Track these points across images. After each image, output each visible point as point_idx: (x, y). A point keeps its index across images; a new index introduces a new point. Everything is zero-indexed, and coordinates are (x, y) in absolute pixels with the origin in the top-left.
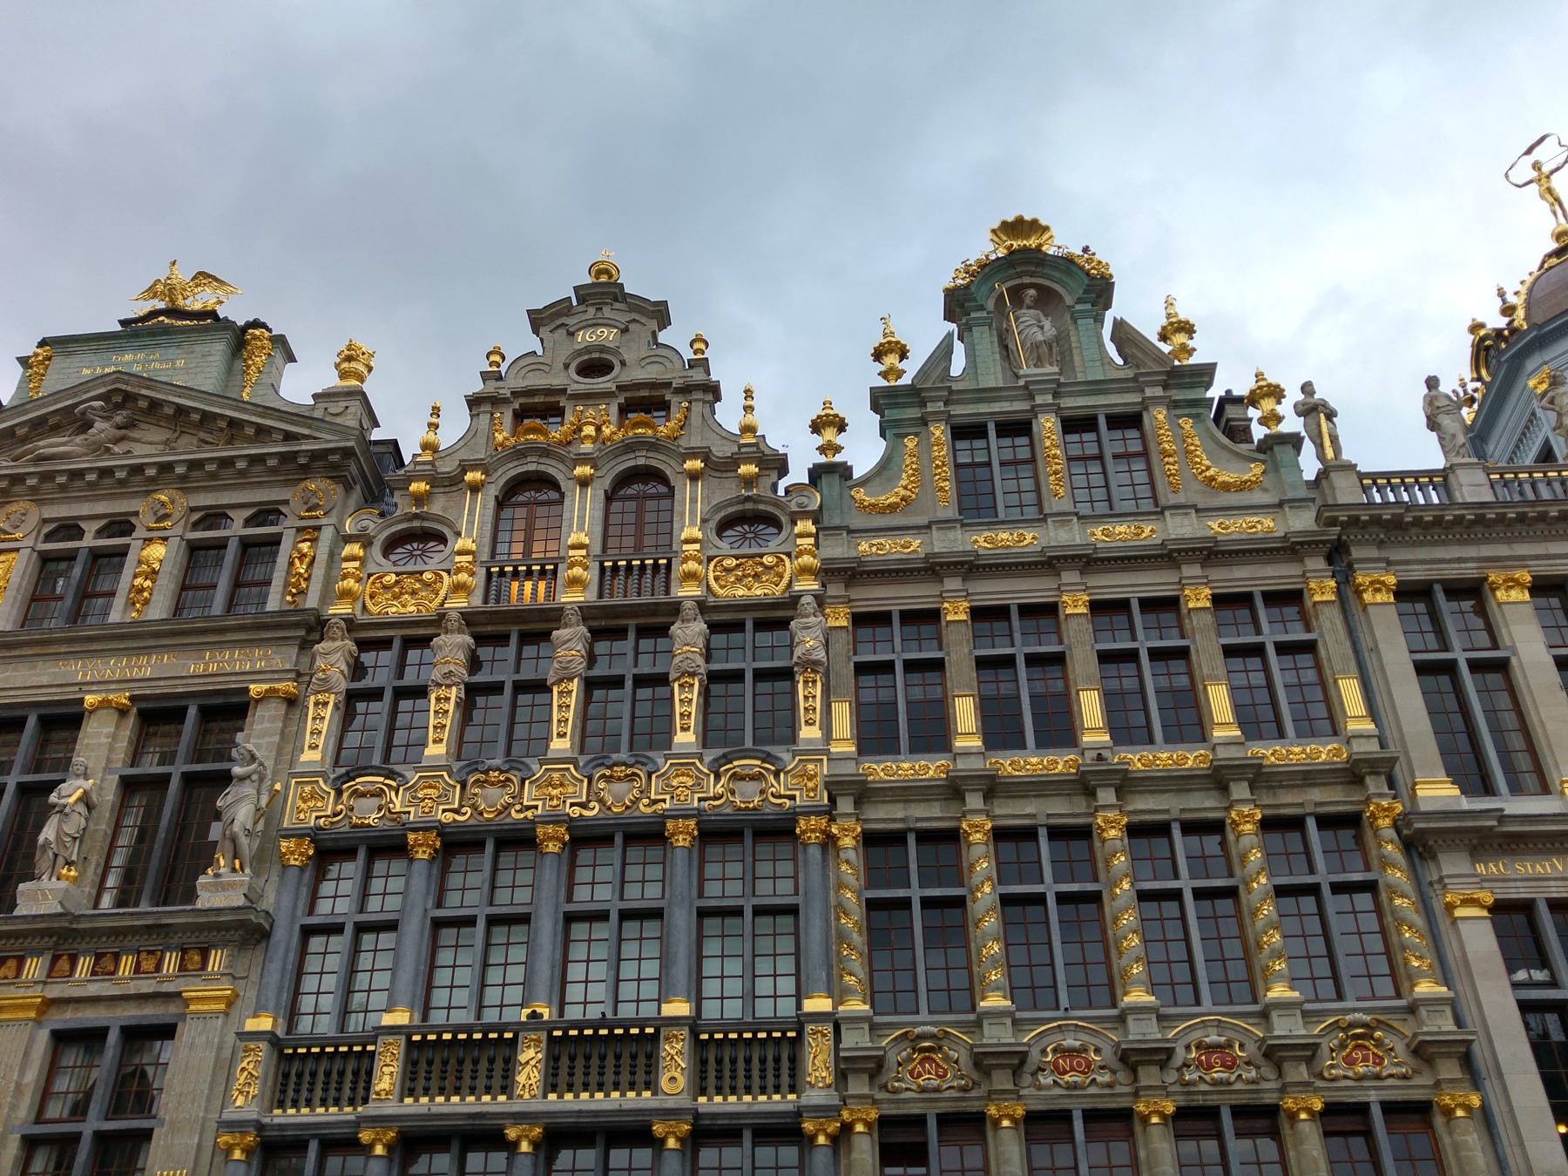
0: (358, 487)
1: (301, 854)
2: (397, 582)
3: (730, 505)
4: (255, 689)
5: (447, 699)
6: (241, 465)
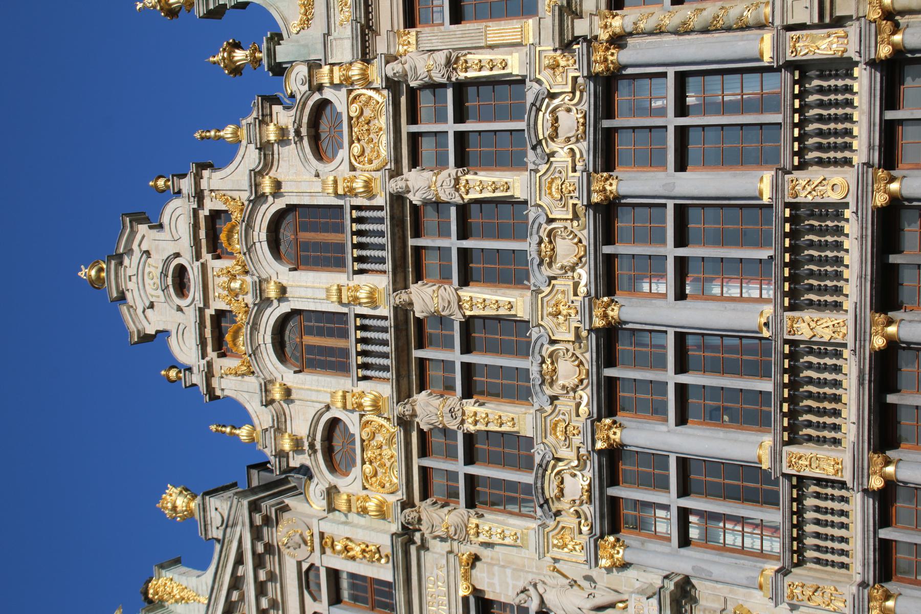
0: (287, 501)
1: (614, 547)
2: (371, 463)
3: (303, 149)
4: (463, 592)
6: (264, 603)
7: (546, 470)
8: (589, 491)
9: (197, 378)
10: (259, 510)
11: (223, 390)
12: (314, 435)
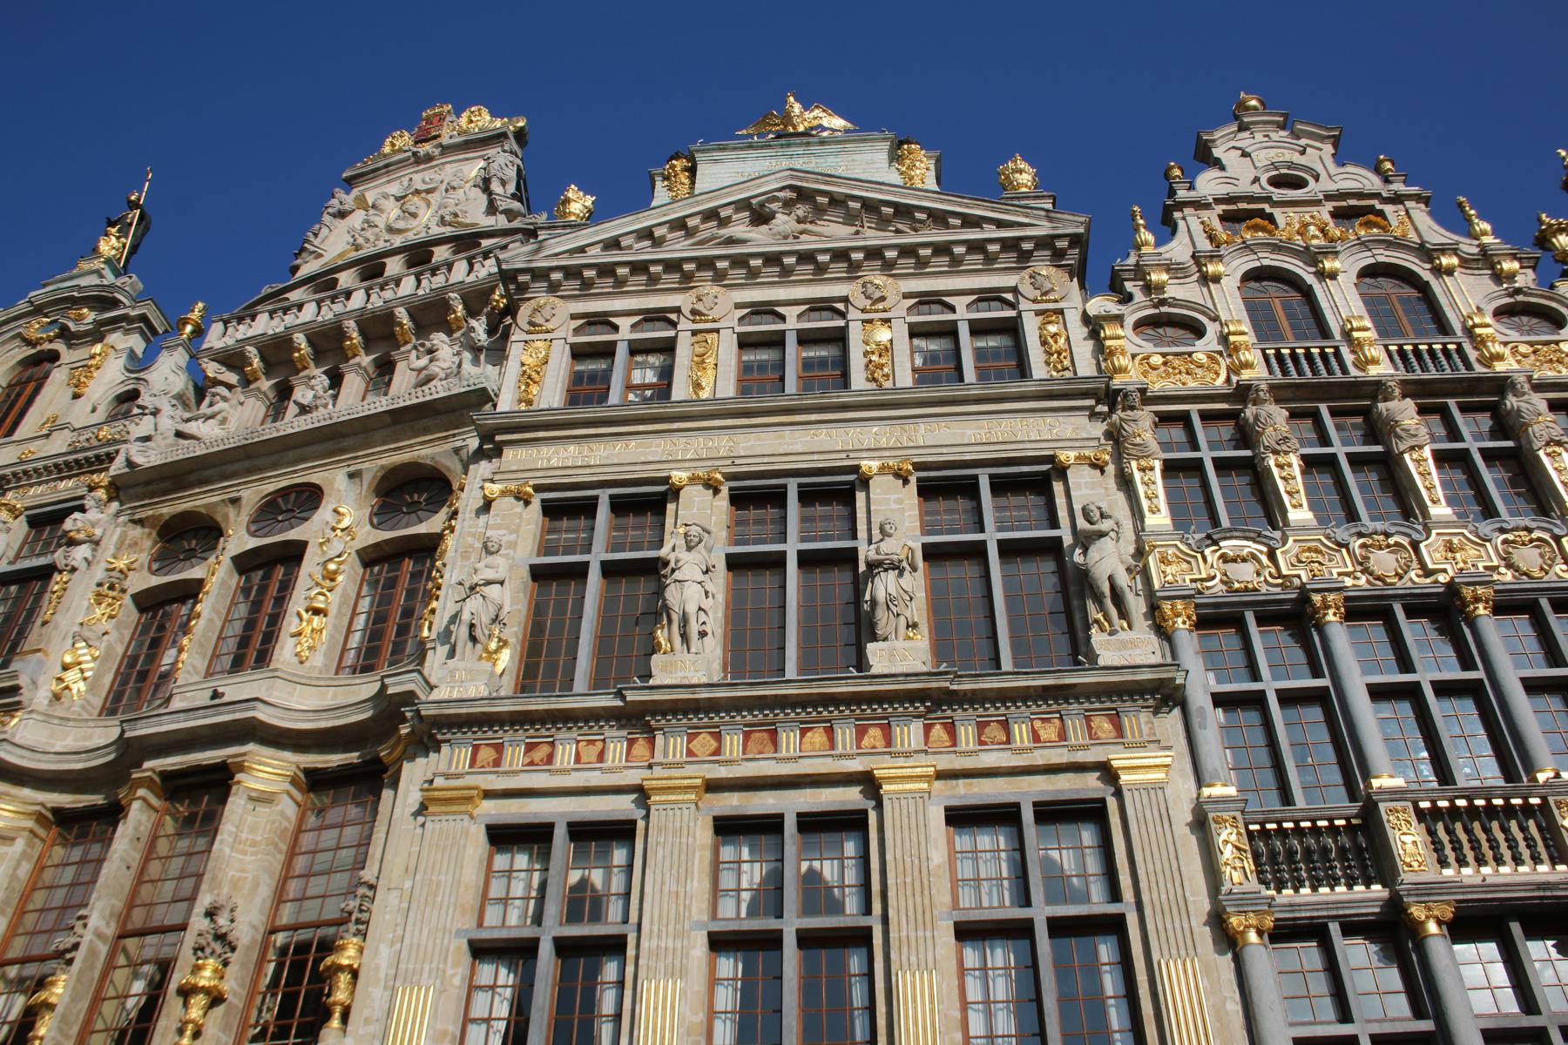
3: (1500, 297)
5: (1290, 465)
7: (1255, 541)
8: (1246, 589)
9: (1182, 194)
10: (1071, 246)
11: (1184, 218)
12: (1174, 306)
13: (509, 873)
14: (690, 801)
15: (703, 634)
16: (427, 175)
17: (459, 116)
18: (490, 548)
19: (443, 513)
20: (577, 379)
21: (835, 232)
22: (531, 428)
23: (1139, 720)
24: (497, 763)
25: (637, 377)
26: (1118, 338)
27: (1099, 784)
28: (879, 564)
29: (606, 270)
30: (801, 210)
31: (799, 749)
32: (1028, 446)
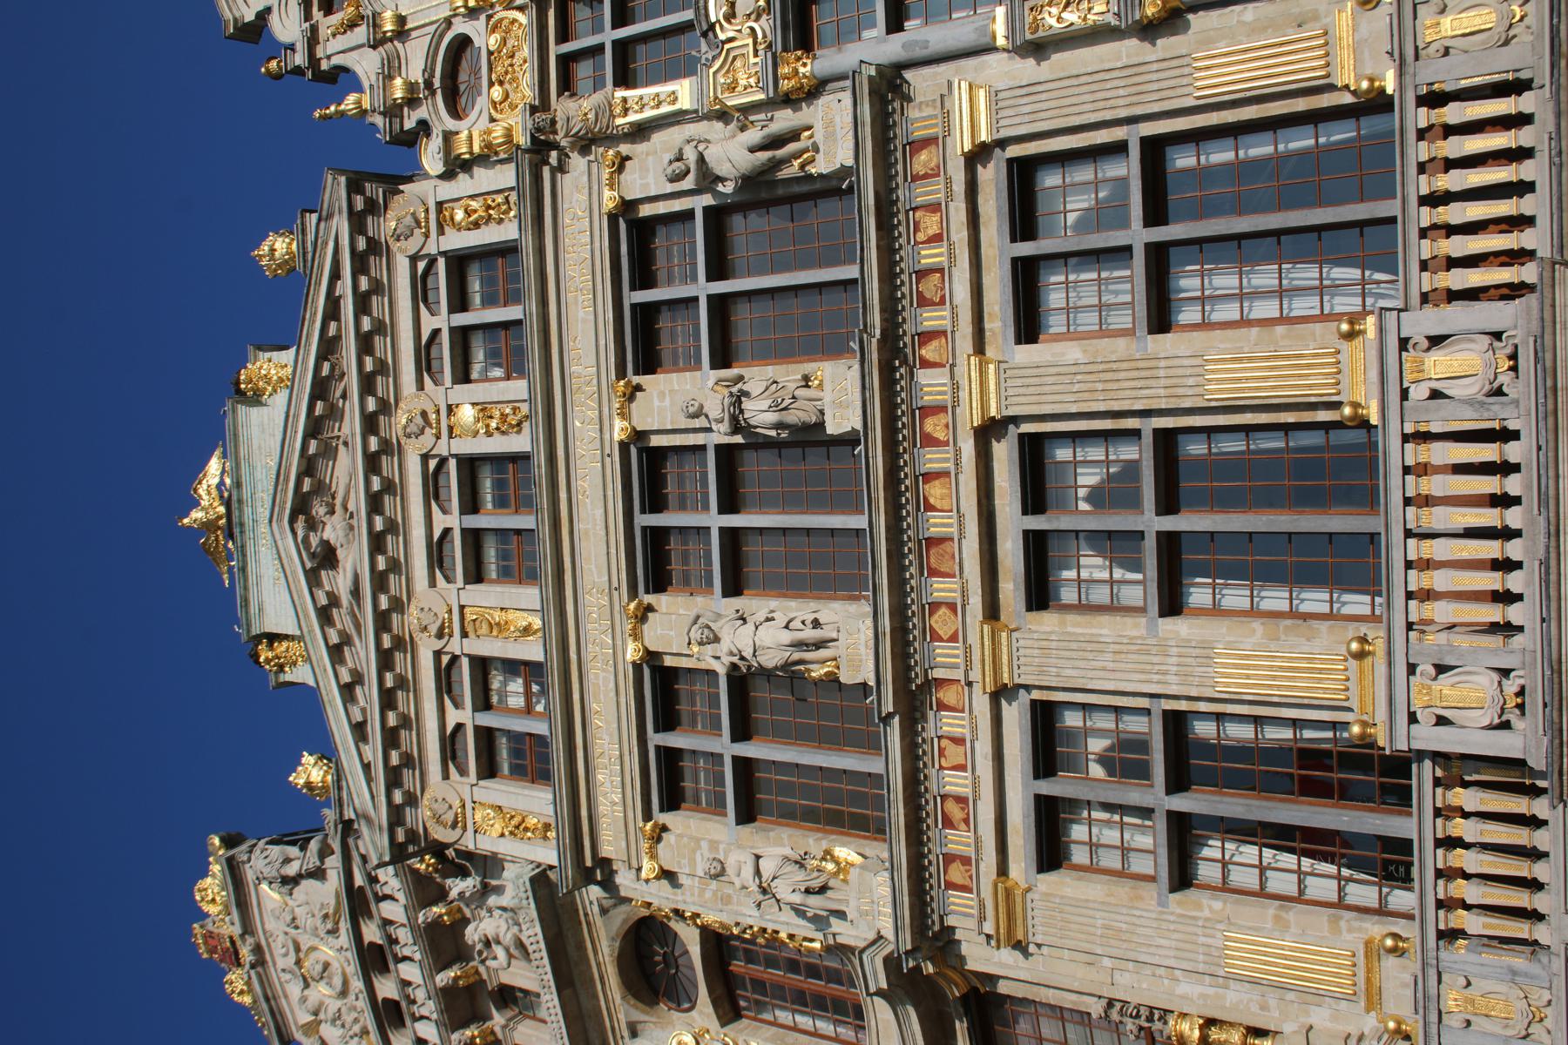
9: (300, 59)
10: (362, 193)
11: (329, 57)
12: (433, 71)
13: (1093, 846)
14: (1009, 638)
15: (816, 624)
16: (278, 950)
17: (207, 915)
18: (717, 874)
19: (676, 926)
20: (518, 772)
21: (346, 470)
22: (576, 825)
23: (917, 119)
24: (966, 861)
25: (516, 701)
26: (470, 138)
27: (991, 165)
28: (734, 419)
29: (391, 738)
30: (319, 510)
31: (949, 513)
32: (597, 244)
